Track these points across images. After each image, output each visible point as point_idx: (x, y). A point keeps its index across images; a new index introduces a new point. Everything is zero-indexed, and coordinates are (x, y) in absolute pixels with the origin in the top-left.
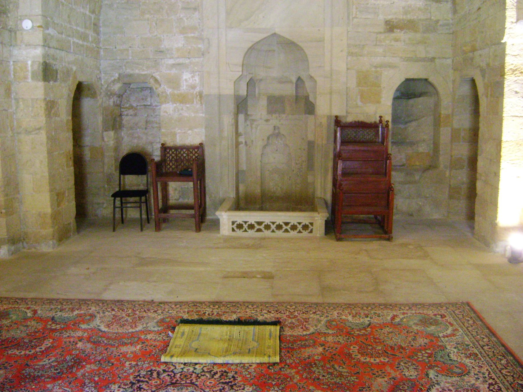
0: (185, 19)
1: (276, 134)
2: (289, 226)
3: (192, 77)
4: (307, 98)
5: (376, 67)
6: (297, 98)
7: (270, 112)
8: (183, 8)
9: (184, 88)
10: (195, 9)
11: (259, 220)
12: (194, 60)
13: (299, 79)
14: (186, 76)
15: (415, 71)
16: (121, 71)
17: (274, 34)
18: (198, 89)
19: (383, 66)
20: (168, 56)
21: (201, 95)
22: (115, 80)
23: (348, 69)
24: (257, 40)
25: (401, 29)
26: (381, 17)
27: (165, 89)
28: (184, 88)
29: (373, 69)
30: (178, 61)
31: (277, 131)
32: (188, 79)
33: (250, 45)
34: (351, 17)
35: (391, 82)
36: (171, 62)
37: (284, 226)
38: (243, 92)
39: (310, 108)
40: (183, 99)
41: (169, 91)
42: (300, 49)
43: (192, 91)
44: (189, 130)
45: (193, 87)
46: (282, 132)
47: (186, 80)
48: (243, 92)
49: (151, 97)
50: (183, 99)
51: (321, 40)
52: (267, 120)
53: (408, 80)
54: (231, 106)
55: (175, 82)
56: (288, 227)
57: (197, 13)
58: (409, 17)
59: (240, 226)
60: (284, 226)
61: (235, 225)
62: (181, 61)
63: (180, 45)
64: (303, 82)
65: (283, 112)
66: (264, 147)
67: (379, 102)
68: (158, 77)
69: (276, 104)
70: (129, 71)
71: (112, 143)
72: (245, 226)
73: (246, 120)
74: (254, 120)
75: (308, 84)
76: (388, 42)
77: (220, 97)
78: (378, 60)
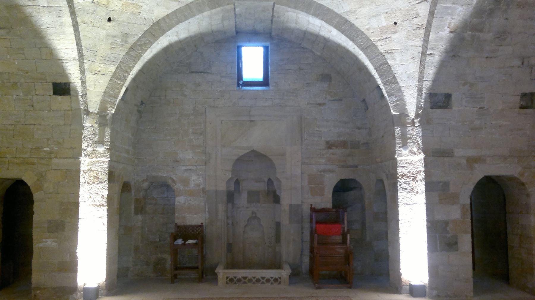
0: (194, 140)
1: (254, 217)
2: (265, 280)
3: (198, 178)
4: (275, 192)
5: (321, 172)
6: (268, 193)
7: (249, 202)
8: (193, 133)
9: (192, 185)
10: (201, 134)
11: (244, 275)
12: (199, 167)
13: (270, 179)
14: (194, 177)
15: (346, 175)
16: (149, 174)
17: (253, 151)
18: (201, 187)
19: (324, 171)
20: (182, 164)
21: (203, 190)
22: (144, 180)
23: (302, 173)
24: (242, 154)
25: (337, 147)
26: (323, 139)
27: (178, 186)
28: (192, 185)
29: (319, 173)
30: (188, 168)
31: (254, 215)
32: (195, 180)
33: (237, 158)
34: (303, 140)
35: (330, 181)
36: (184, 168)
37: (261, 279)
38: (232, 188)
39: (277, 200)
40: (191, 193)
41: (182, 188)
42: (270, 160)
43: (198, 188)
44: (195, 214)
45: (199, 185)
46: (258, 216)
47: (193, 180)
48: (232, 188)
49: (167, 191)
50: (191, 193)
51: (284, 154)
52: (247, 208)
53: (342, 180)
54: (225, 198)
55: (186, 182)
56: (264, 281)
57: (202, 136)
58: (341, 139)
59: (231, 280)
60: (261, 279)
61: (228, 279)
62: (190, 167)
63: (190, 157)
64: (272, 182)
65: (259, 202)
66: (246, 226)
67: (323, 195)
68: (174, 178)
69: (253, 196)
70: (154, 174)
71: (139, 224)
72: (235, 280)
73: (233, 208)
74: (239, 208)
75: (275, 183)
76: (328, 155)
77: (216, 192)
78: (322, 167)
